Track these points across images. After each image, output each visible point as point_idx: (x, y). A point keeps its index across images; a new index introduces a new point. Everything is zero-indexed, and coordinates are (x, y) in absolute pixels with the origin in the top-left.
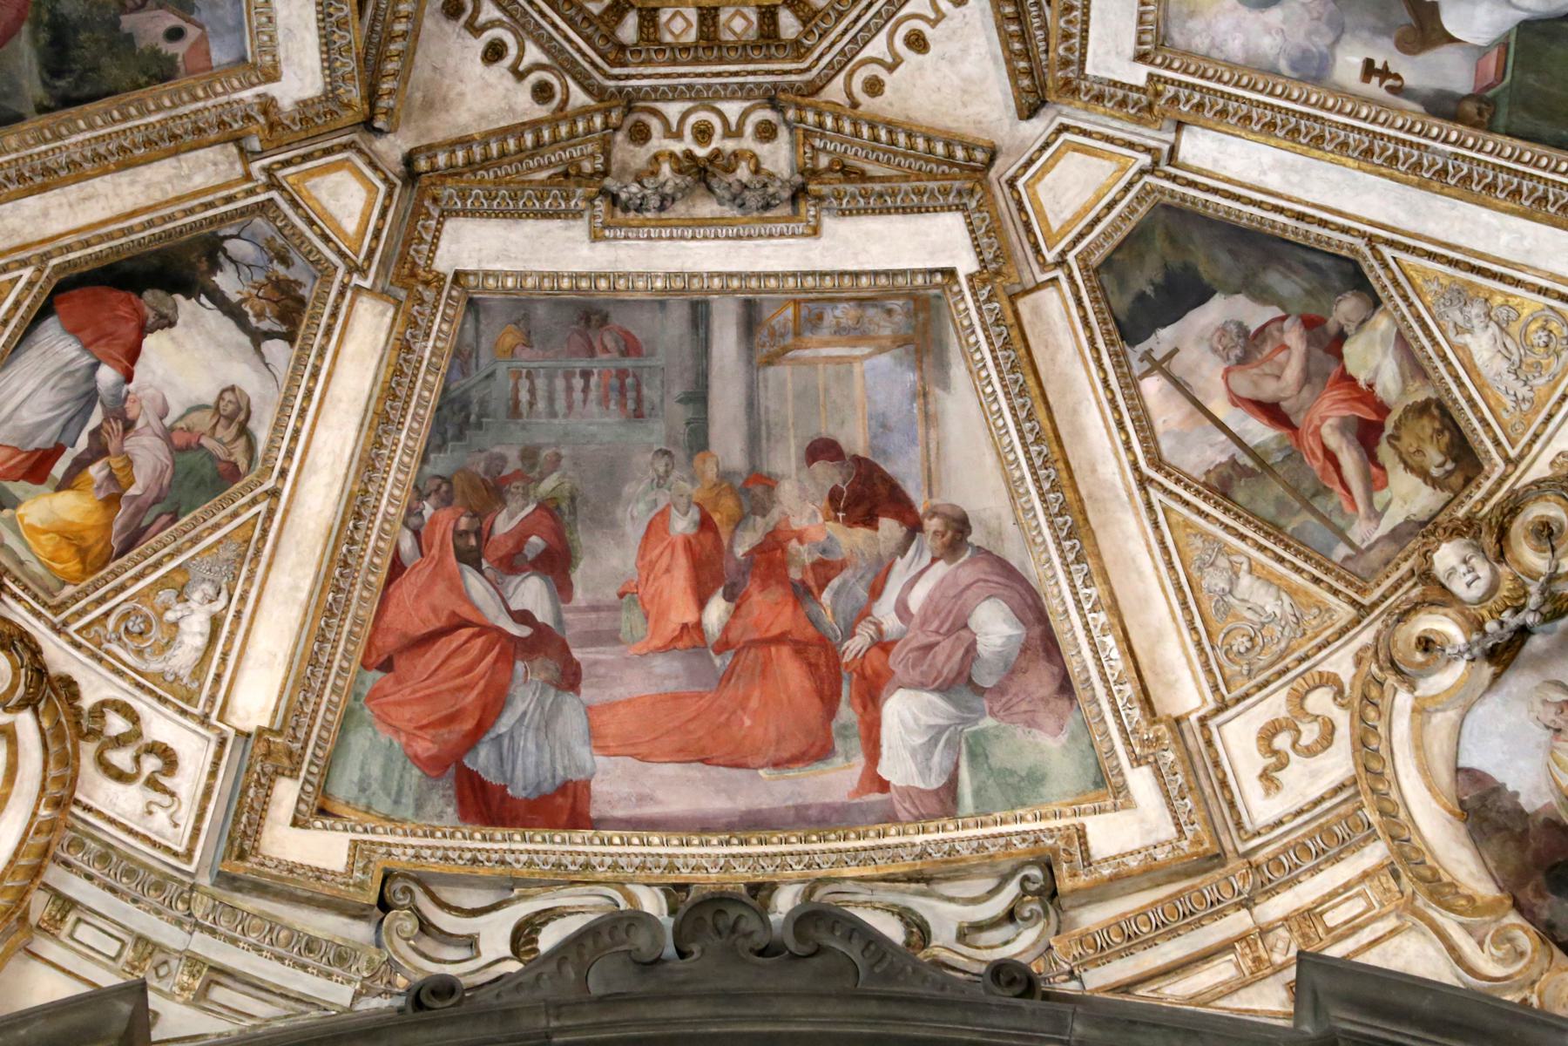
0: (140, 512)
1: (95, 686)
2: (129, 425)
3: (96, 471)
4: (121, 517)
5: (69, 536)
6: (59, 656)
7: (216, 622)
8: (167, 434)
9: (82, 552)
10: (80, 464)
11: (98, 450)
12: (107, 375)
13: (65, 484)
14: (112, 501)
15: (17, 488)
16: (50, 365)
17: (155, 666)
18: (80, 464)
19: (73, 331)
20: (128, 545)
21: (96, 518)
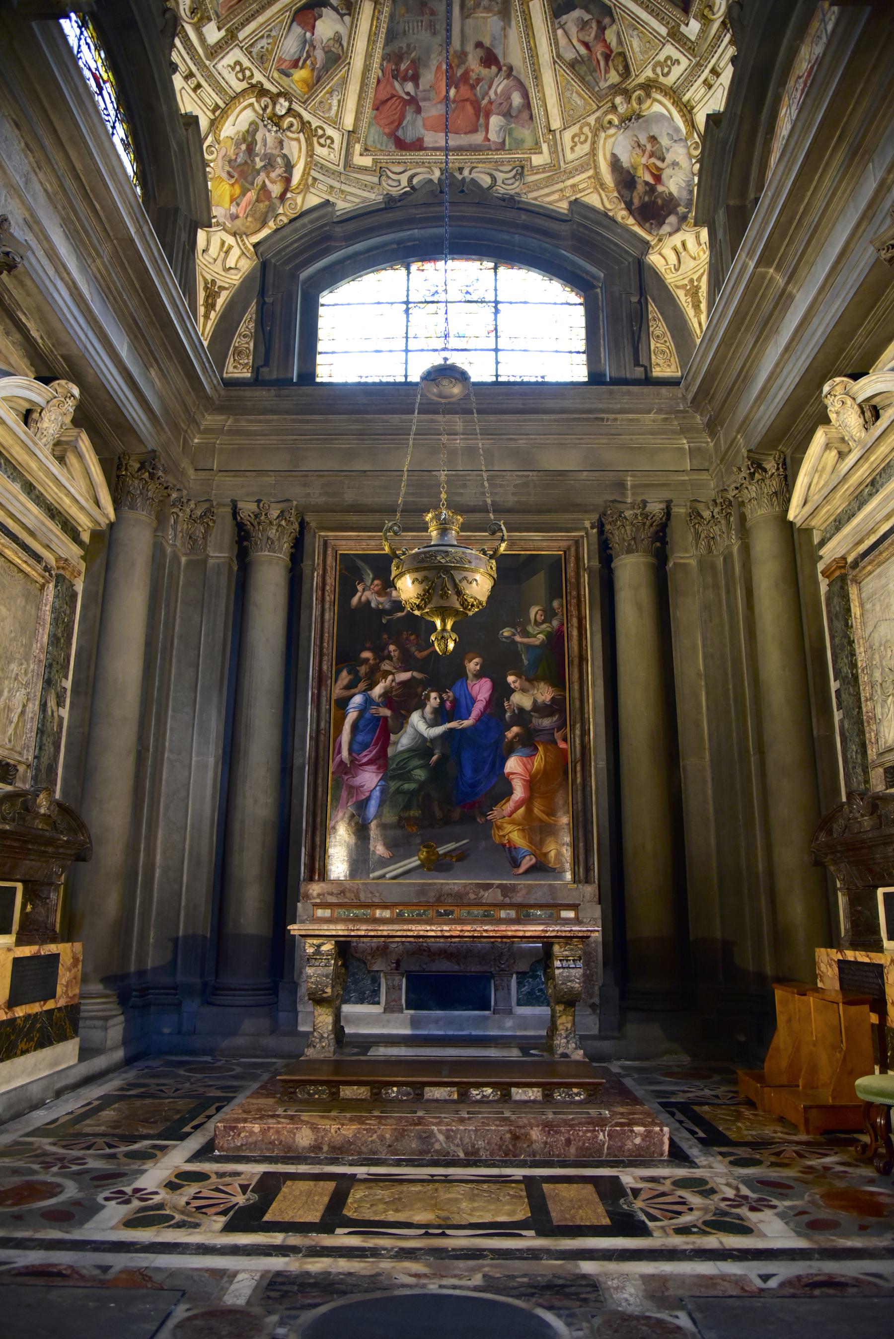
0: (319, 72)
1: (315, 123)
2: (314, 47)
3: (308, 62)
4: (315, 74)
5: (304, 81)
6: (306, 116)
7: (339, 101)
8: (323, 48)
9: (308, 85)
10: (305, 61)
11: (308, 57)
12: (308, 35)
13: (302, 68)
14: (313, 70)
15: (292, 71)
16: (296, 35)
17: (327, 115)
18: (305, 61)
19: (299, 25)
20: (318, 81)
21: (310, 75)
